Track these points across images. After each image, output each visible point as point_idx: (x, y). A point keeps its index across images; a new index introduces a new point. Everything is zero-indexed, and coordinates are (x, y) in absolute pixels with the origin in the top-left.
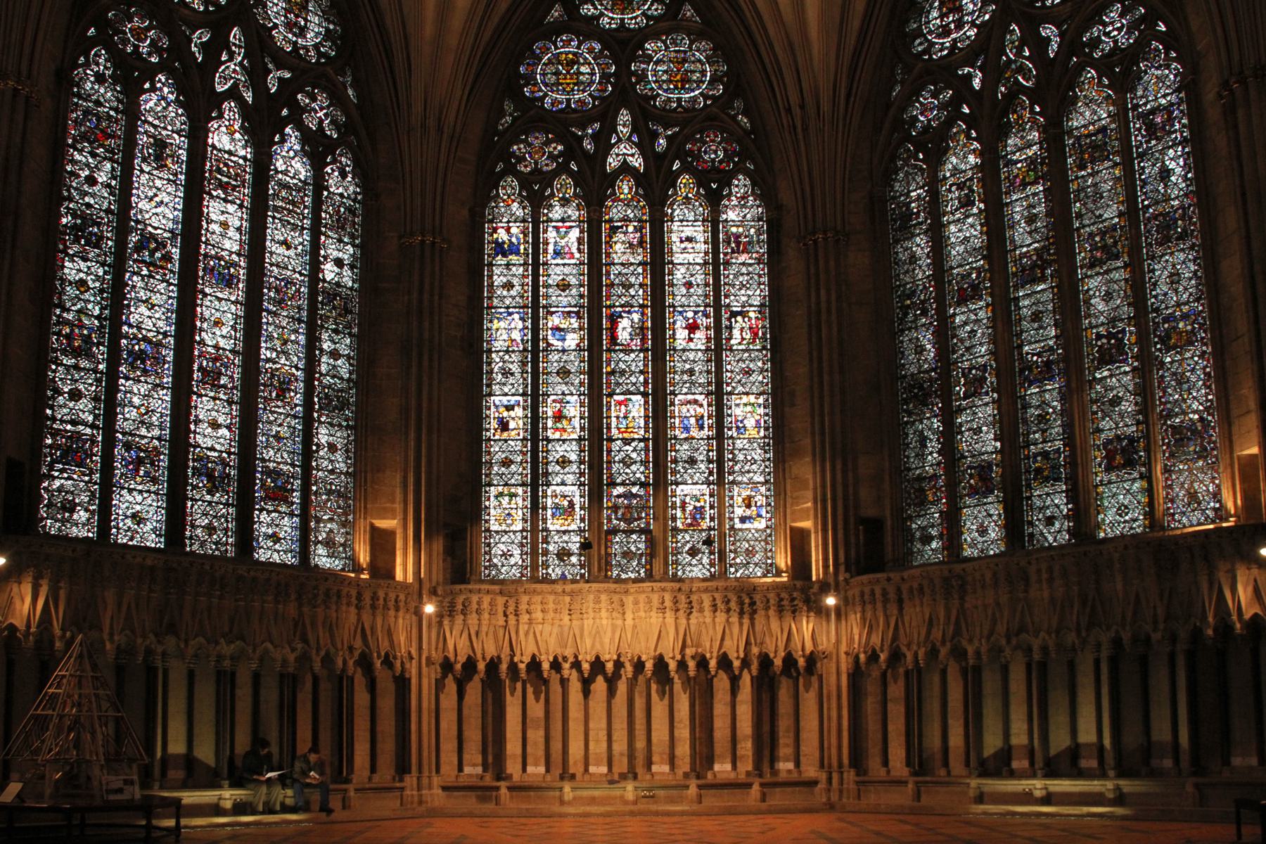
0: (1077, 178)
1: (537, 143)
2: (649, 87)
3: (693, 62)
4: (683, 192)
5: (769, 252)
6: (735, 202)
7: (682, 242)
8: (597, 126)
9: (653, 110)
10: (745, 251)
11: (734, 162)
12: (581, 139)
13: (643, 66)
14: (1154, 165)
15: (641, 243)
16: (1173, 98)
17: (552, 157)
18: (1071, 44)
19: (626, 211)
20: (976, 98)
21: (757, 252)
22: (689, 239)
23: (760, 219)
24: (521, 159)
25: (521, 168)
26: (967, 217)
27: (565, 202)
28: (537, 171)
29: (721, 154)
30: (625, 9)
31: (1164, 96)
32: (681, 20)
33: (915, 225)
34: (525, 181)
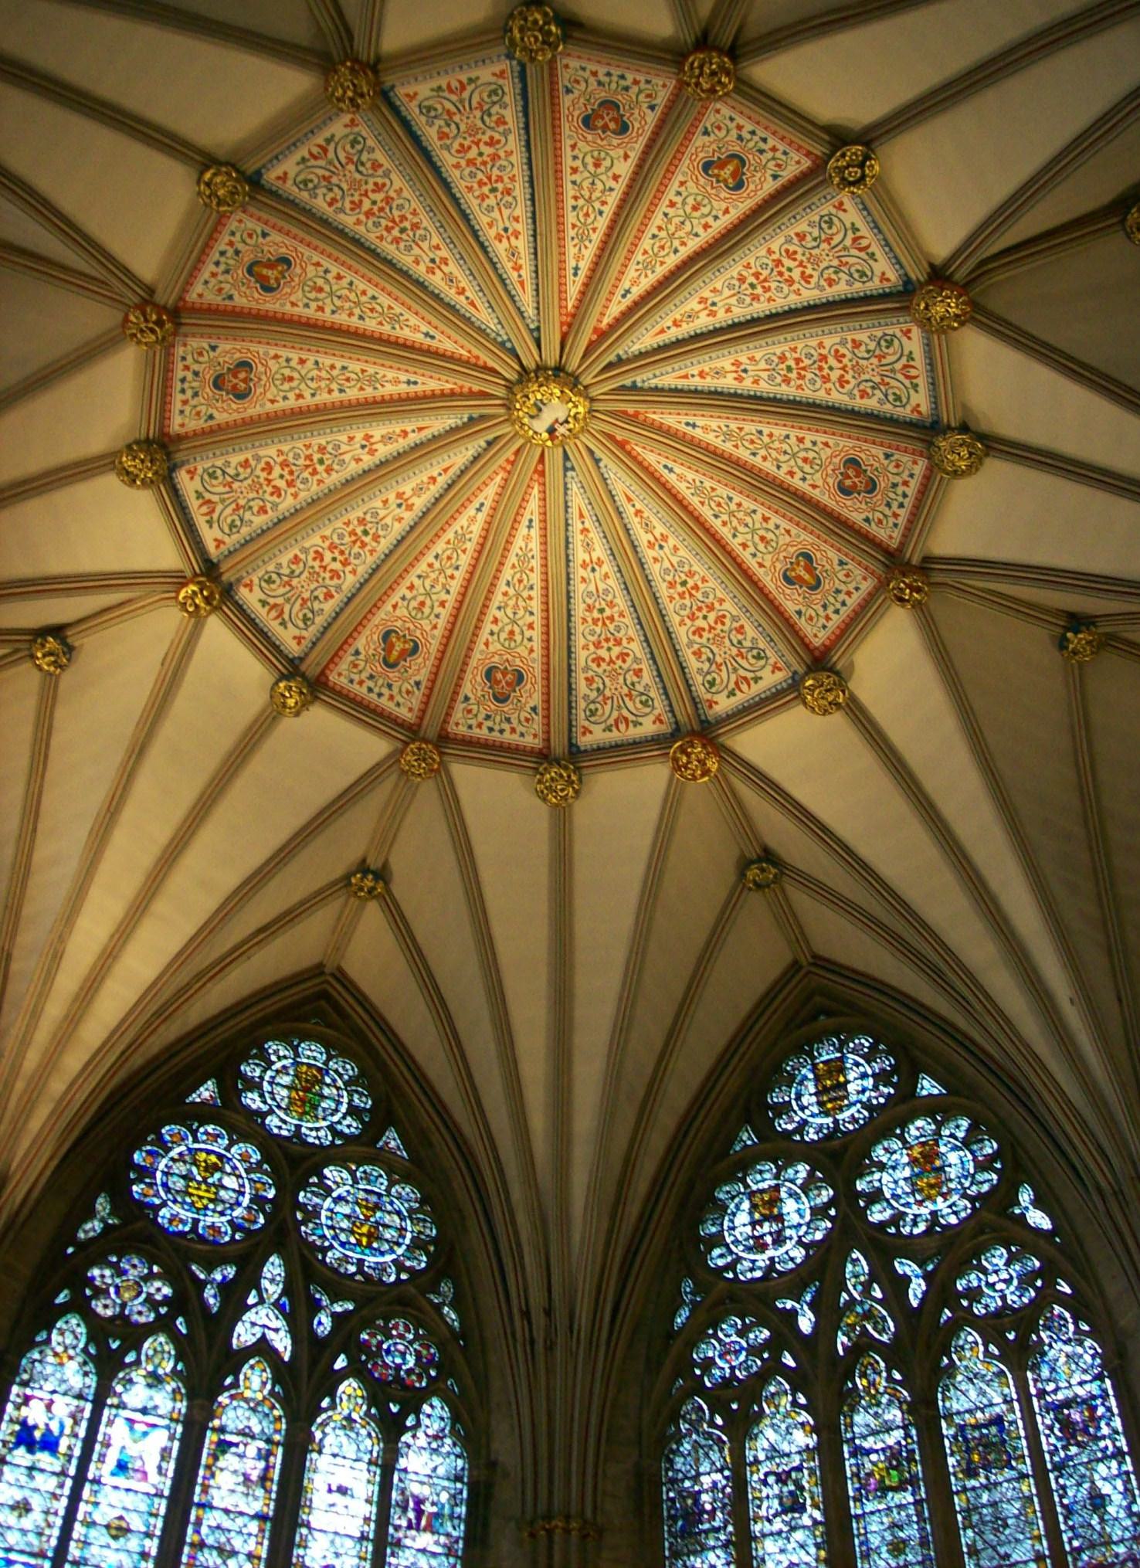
0: (965, 1489)
1: (133, 1274)
2: (319, 1232)
3: (389, 1213)
4: (345, 1407)
5: (468, 1539)
6: (422, 1441)
7: (330, 1491)
8: (231, 1271)
9: (319, 1266)
10: (430, 1528)
11: (429, 1376)
12: (202, 1285)
13: (316, 1200)
14: (1079, 1484)
15: (264, 1479)
16: (1094, 1388)
17: (150, 1300)
18: (941, 1290)
19: (248, 1419)
20: (804, 1345)
21: (448, 1535)
22: (342, 1490)
23: (458, 1478)
24: (101, 1292)
25: (98, 1306)
26: (793, 1529)
27: (155, 1380)
28: (122, 1318)
29: (411, 1361)
30: (305, 1113)
31: (1081, 1383)
32: (381, 1148)
33: (706, 1532)
34: (98, 1330)
